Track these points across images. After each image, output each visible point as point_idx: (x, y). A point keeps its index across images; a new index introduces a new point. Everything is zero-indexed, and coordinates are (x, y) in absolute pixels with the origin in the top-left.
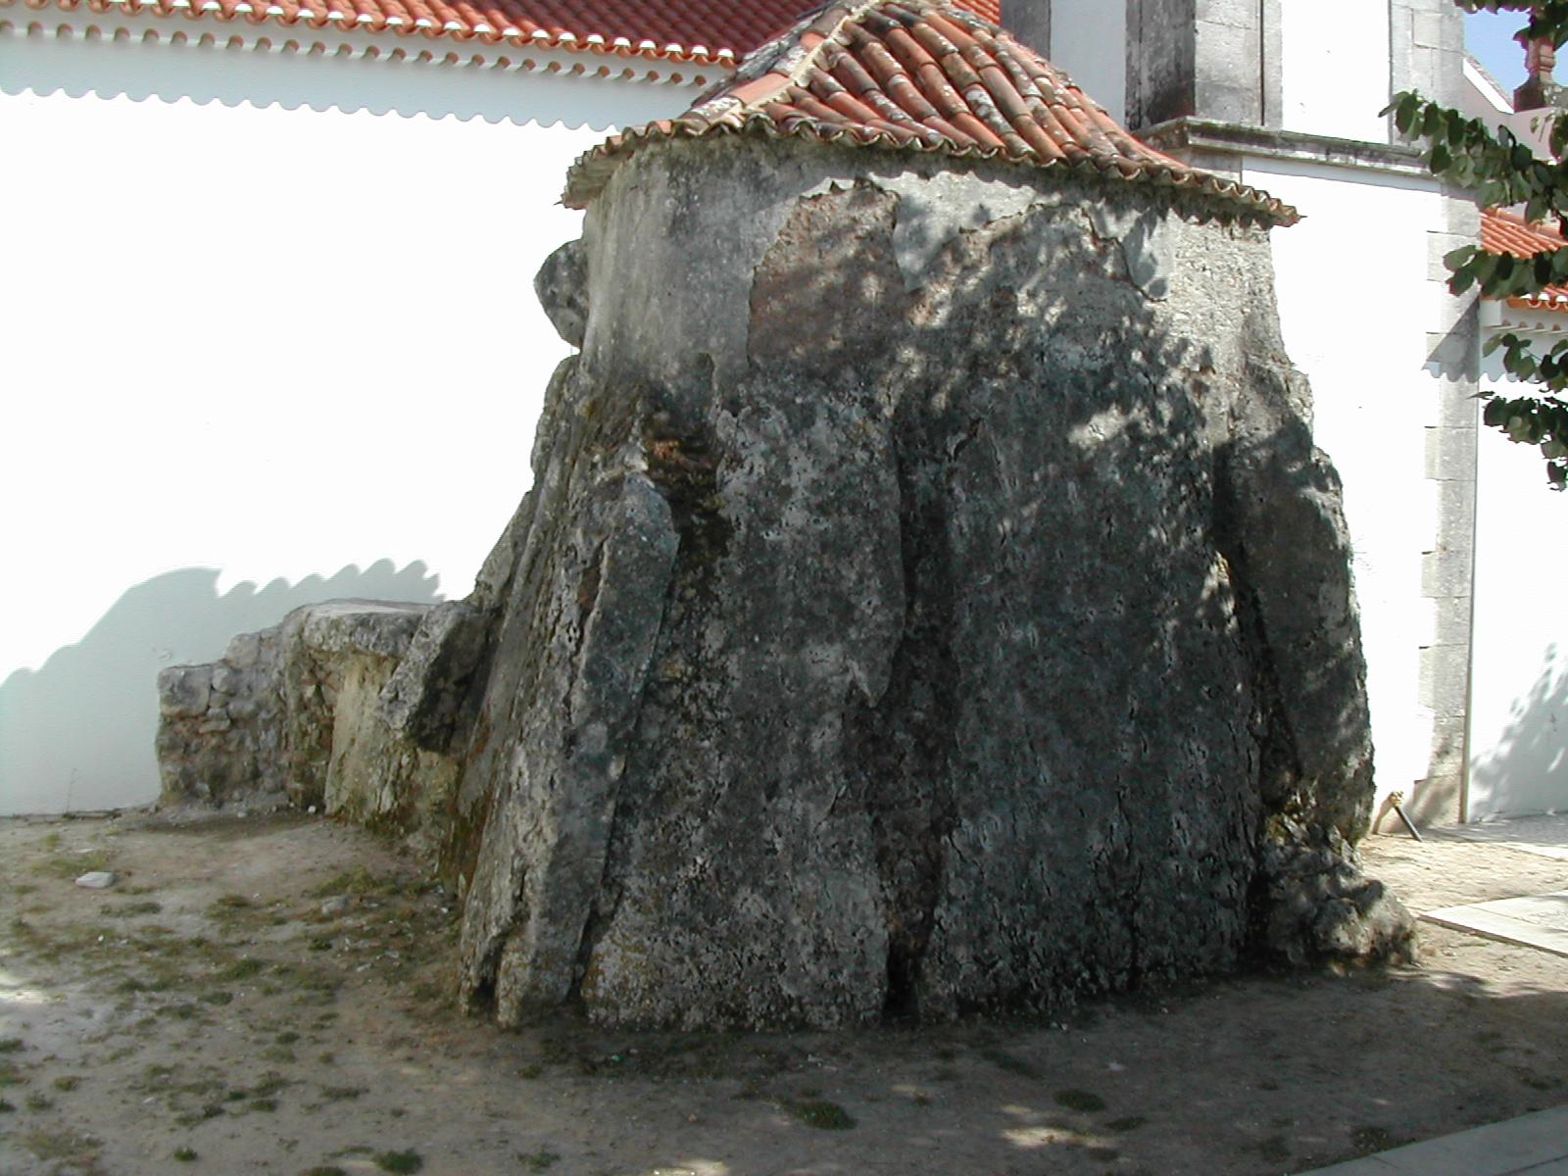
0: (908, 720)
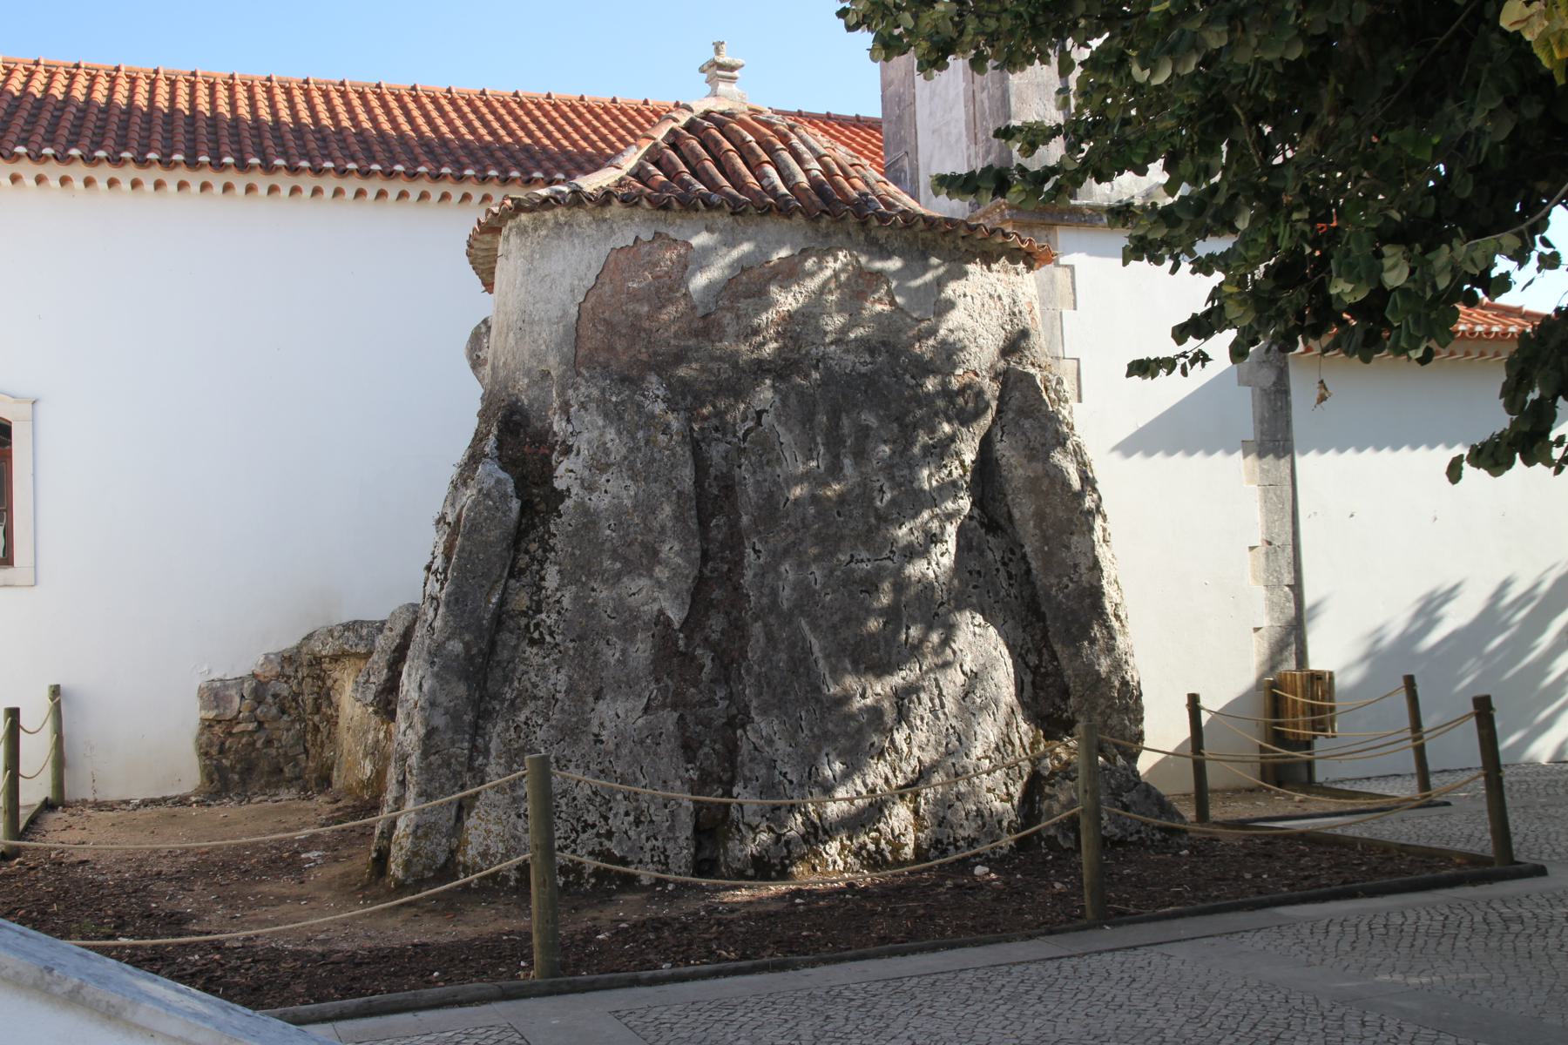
0: (706, 639)
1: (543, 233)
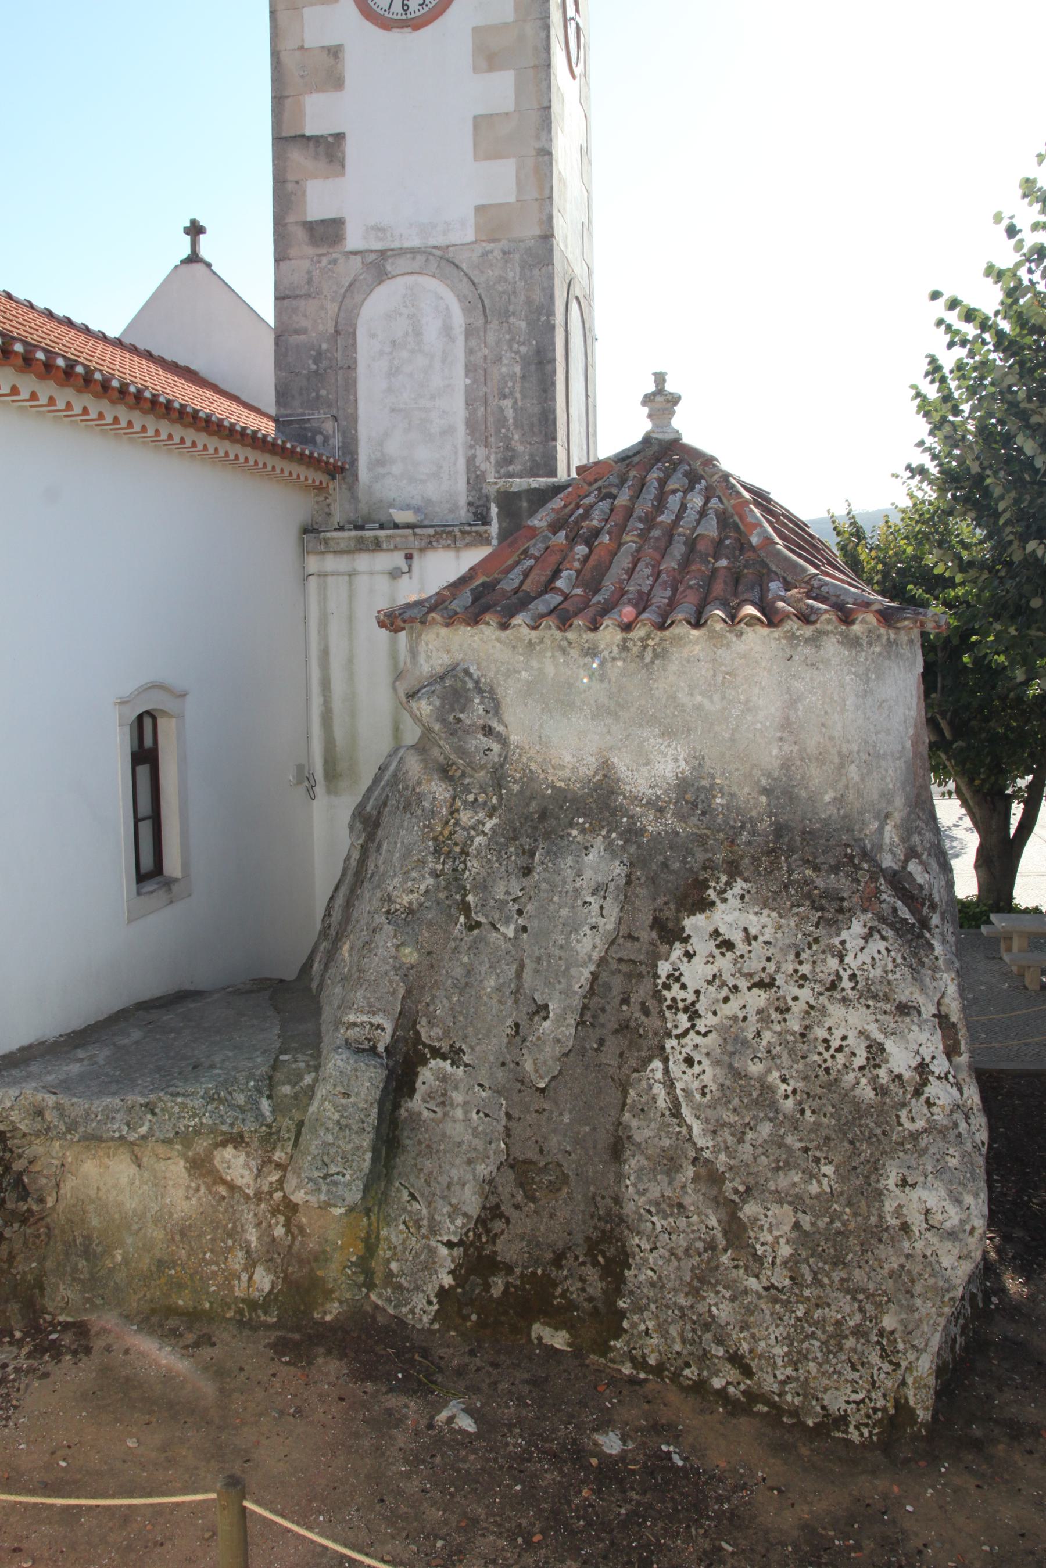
1: (878, 649)
